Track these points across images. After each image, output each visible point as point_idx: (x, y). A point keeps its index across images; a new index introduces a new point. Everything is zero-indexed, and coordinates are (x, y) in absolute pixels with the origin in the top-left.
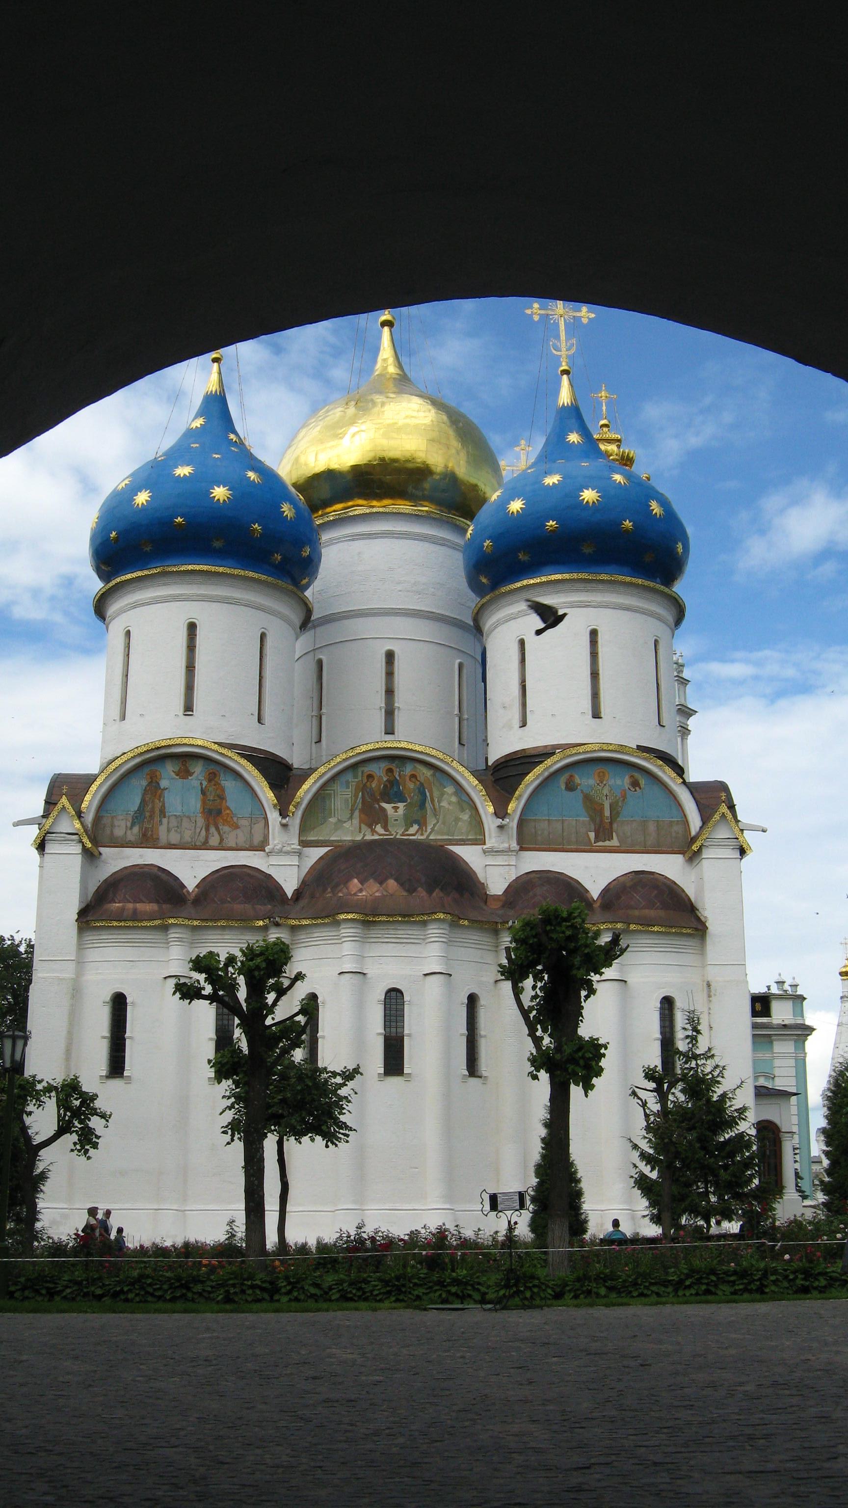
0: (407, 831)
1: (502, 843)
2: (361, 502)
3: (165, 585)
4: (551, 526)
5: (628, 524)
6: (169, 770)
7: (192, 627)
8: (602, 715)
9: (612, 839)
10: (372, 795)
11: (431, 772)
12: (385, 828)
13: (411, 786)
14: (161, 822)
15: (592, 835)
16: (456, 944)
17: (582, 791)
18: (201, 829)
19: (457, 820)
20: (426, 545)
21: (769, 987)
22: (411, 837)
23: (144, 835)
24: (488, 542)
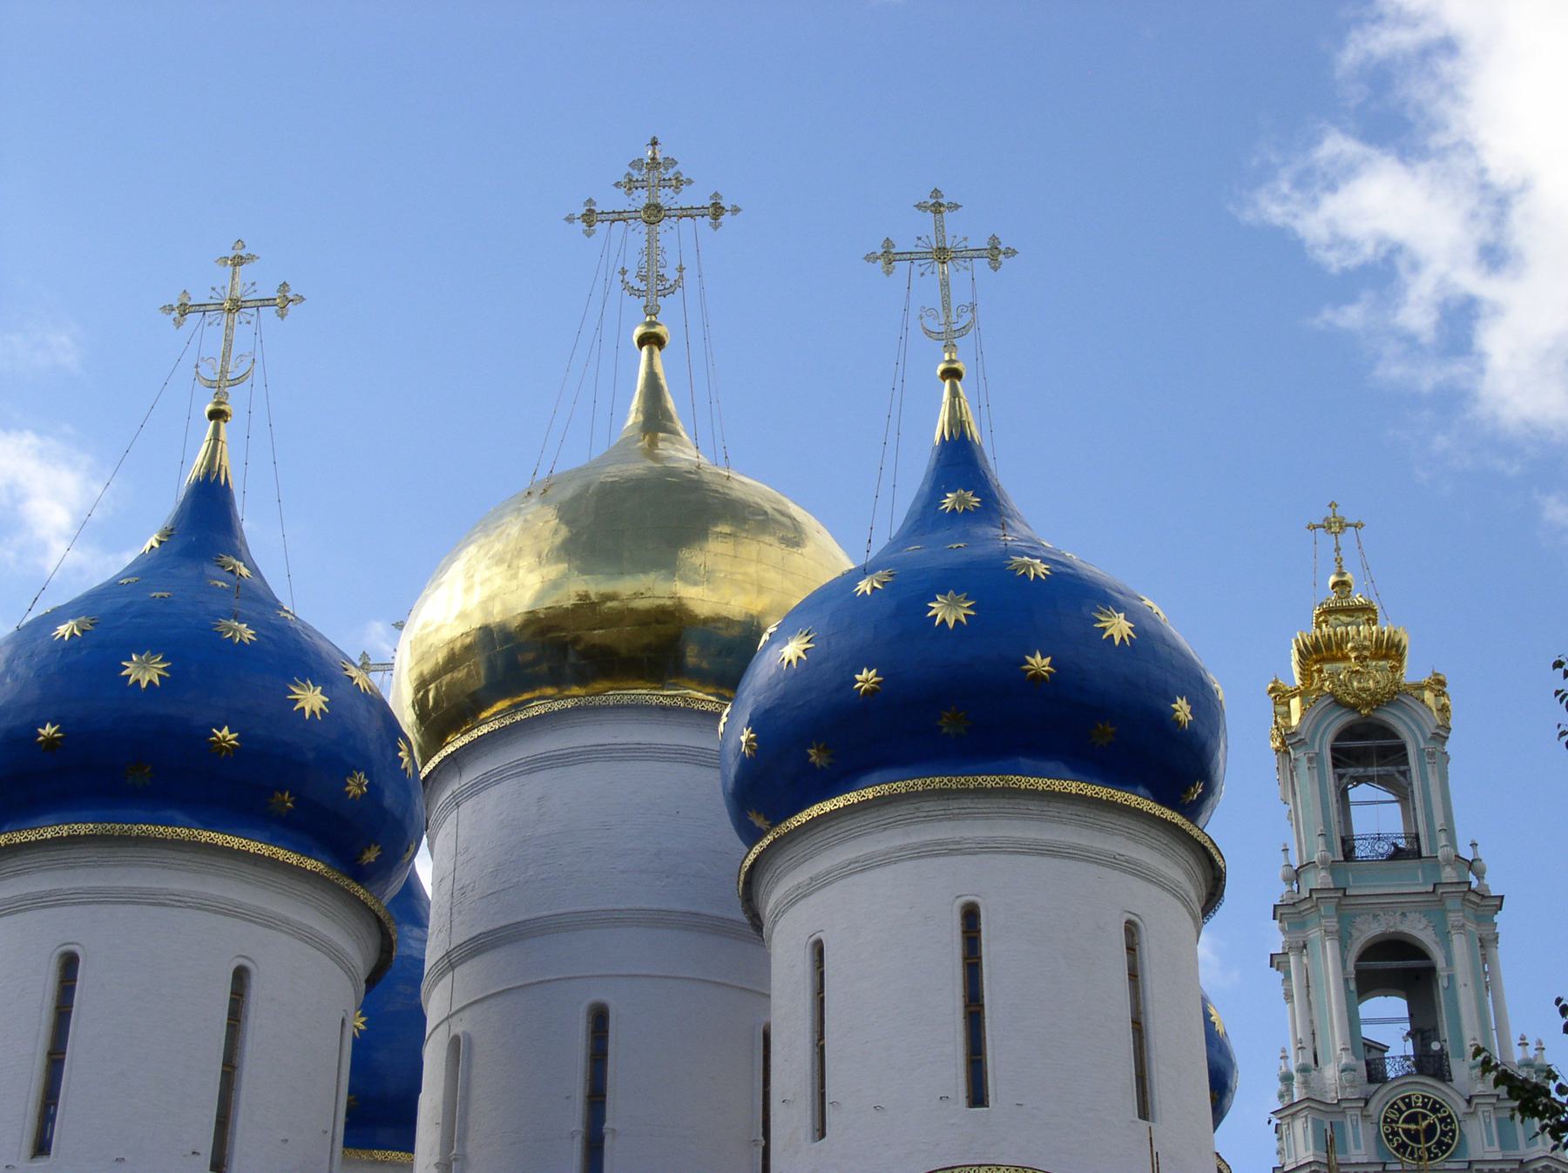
2: (550, 691)
3: (16, 874)
4: (866, 681)
7: (69, 964)
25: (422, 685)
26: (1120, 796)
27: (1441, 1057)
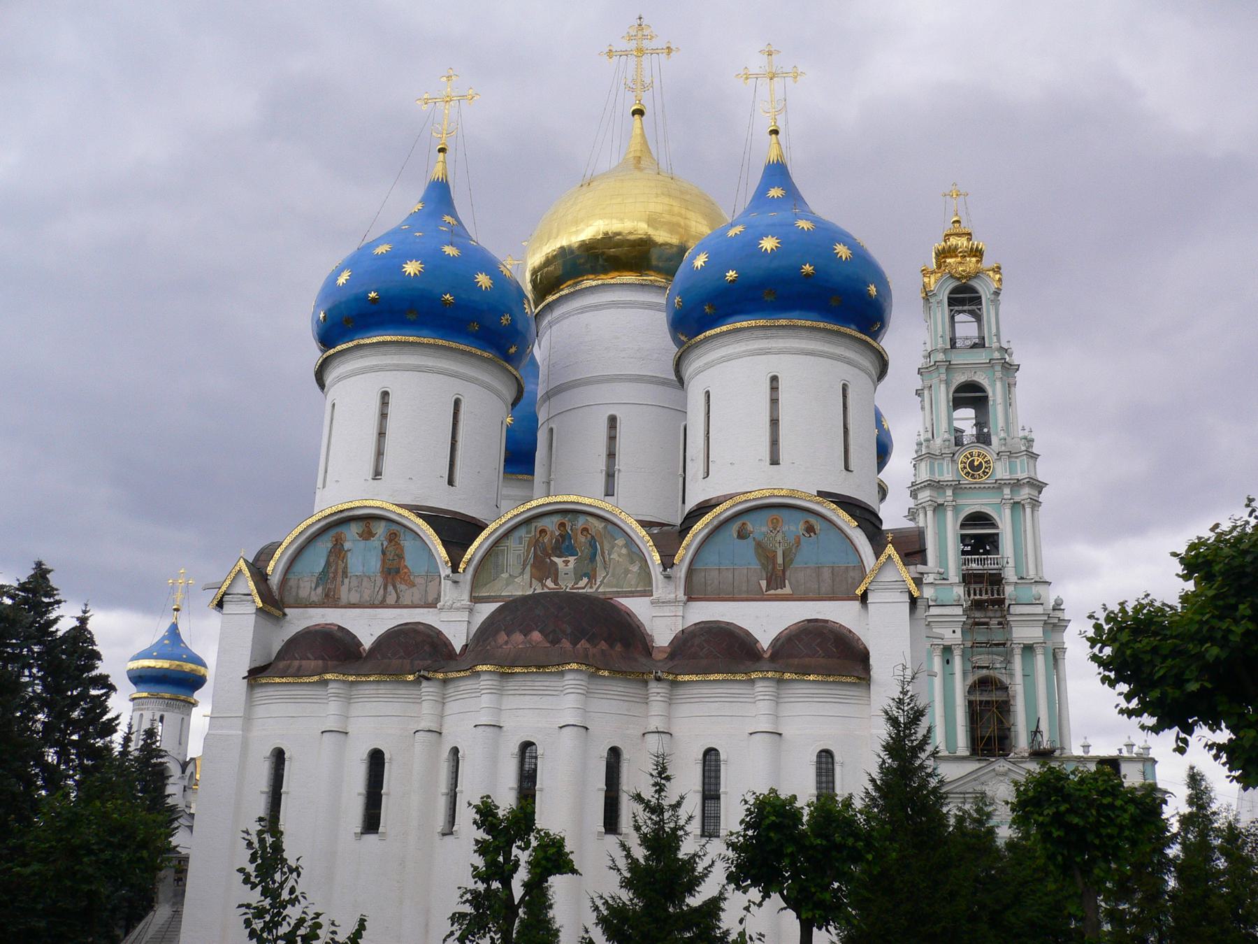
0: (577, 584)
1: (669, 594)
2: (591, 277)
4: (731, 276)
5: (807, 268)
6: (354, 530)
7: (385, 395)
8: (781, 462)
9: (785, 587)
10: (544, 550)
11: (603, 524)
12: (555, 582)
13: (582, 539)
14: (343, 582)
15: (764, 583)
16: (596, 695)
17: (754, 538)
18: (380, 588)
19: (627, 572)
20: (652, 312)
21: (1120, 750)
22: (580, 591)
23: (327, 595)
24: (677, 298)
25: (534, 272)
26: (843, 329)
27: (989, 435)
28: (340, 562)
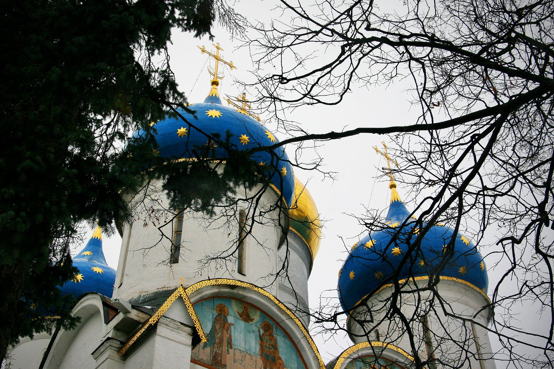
28: (225, 332)
